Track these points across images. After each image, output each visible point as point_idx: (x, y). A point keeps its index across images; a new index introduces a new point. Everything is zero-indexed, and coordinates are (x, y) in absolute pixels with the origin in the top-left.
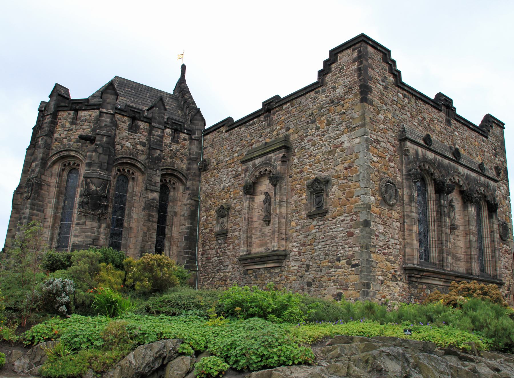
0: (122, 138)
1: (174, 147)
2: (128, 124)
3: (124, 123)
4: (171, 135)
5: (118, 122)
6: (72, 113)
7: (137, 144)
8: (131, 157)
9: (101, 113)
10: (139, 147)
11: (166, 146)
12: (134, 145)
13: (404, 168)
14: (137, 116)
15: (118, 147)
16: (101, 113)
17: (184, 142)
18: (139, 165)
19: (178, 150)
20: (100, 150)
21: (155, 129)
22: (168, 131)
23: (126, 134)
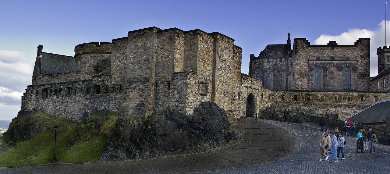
9: (260, 60)
18: (271, 71)
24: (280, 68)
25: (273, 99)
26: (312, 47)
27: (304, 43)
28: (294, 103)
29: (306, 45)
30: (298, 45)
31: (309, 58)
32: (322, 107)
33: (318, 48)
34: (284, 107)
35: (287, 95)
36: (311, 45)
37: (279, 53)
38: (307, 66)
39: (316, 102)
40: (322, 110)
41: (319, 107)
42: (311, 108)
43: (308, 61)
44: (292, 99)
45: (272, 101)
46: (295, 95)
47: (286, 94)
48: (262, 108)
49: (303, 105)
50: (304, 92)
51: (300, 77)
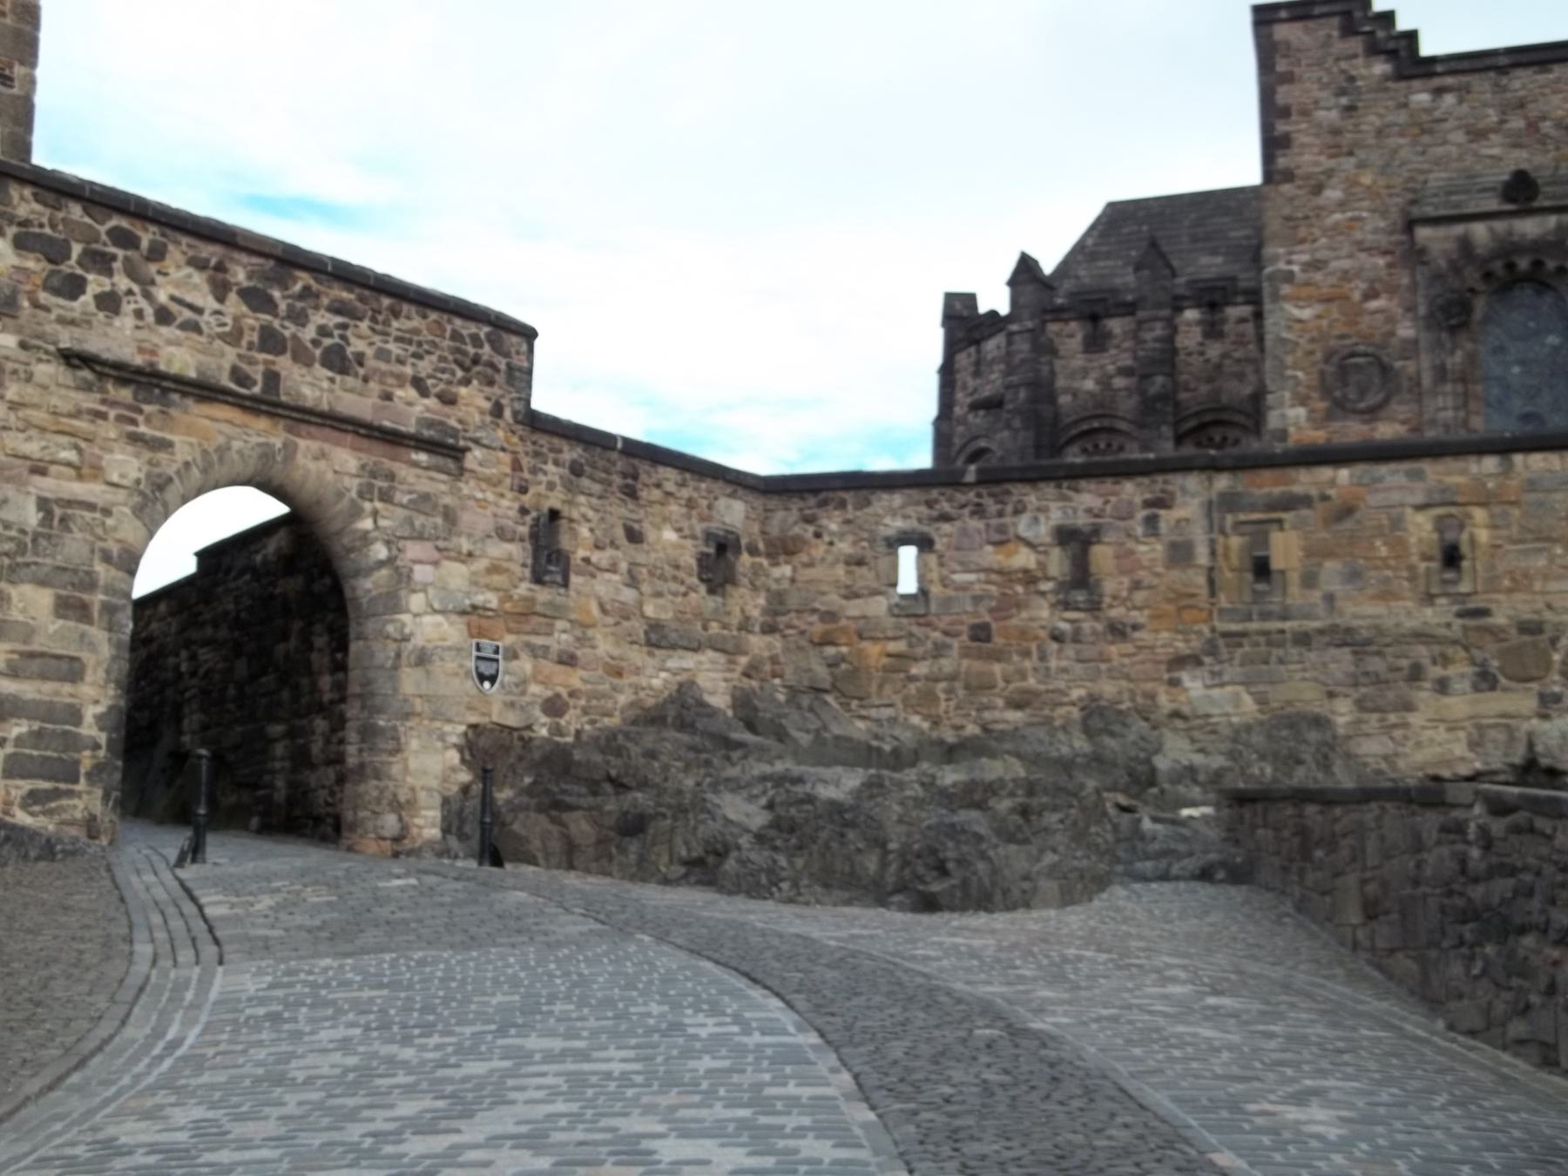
0: (1072, 375)
1: (1214, 350)
2: (1079, 337)
3: (1070, 336)
4: (1199, 323)
5: (1056, 340)
6: (972, 350)
7: (1111, 377)
8: (1100, 411)
9: (1010, 335)
10: (1119, 382)
11: (1190, 354)
12: (1105, 382)
13: (1421, 300)
14: (1098, 309)
15: (1064, 400)
16: (1010, 335)
17: (1241, 327)
18: (1123, 426)
19: (1225, 355)
20: (1017, 423)
21: (1145, 326)
22: (1191, 314)
23: (1079, 361)
24: (1204, 389)
25: (777, 603)
26: (1449, 81)
27: (1356, 44)
28: (1057, 637)
29: (1381, 68)
30: (1289, 78)
31: (1413, 202)
32: (1460, 671)
33: (1521, 82)
34: (928, 697)
35: (964, 532)
36: (1433, 60)
37: (1205, 260)
38: (1392, 290)
39: (1361, 611)
40: (1460, 704)
41: (1416, 674)
42: (1300, 686)
43: (1410, 225)
44: (1029, 578)
45: (769, 629)
46: (1064, 535)
47: (945, 518)
48: (554, 707)
49: (1179, 662)
50: (1192, 481)
51: (1329, 416)
